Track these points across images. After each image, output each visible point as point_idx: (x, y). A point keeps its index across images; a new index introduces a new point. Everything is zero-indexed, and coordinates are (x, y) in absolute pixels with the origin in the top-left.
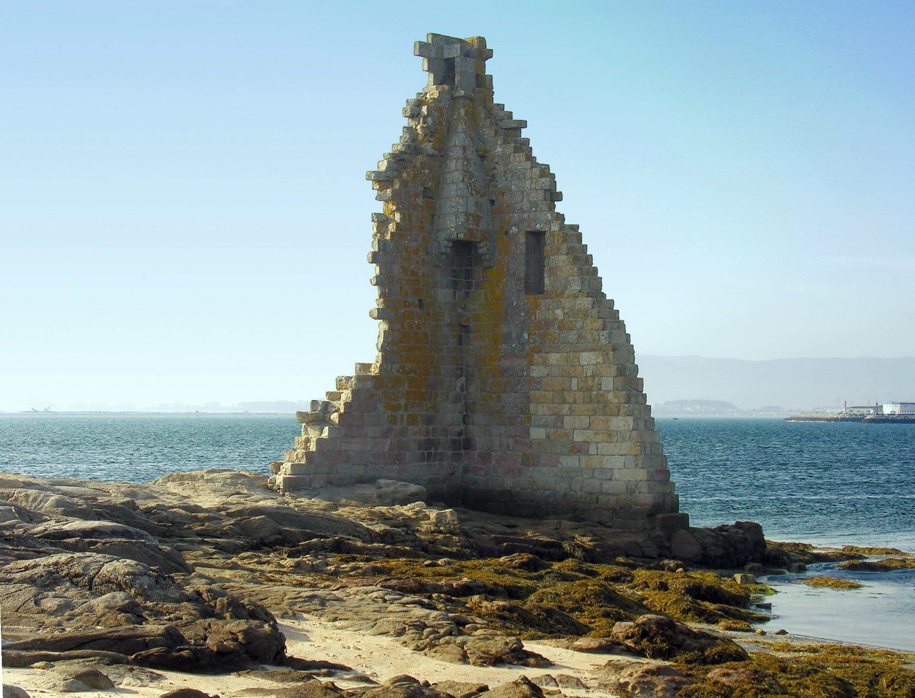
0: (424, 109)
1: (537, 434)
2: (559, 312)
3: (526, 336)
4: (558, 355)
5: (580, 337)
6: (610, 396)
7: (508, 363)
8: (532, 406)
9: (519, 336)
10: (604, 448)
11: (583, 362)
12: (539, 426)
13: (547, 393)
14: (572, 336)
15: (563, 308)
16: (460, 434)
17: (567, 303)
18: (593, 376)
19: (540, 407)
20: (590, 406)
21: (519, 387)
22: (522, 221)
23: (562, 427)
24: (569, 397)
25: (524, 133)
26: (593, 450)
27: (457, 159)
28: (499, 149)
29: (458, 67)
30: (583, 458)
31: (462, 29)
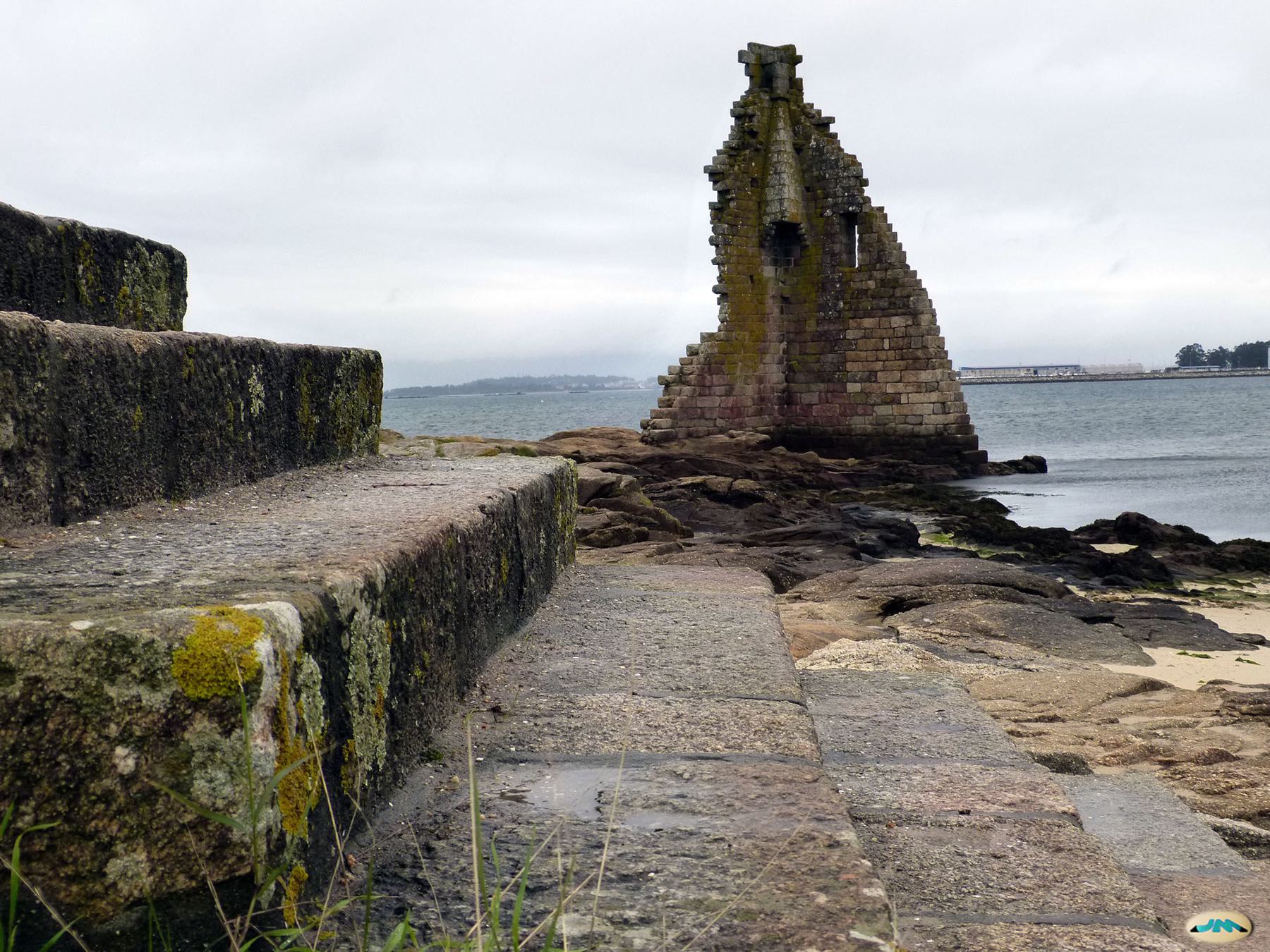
1: (853, 387)
5: (890, 304)
9: (836, 305)
10: (915, 397)
11: (894, 325)
14: (884, 303)
16: (783, 391)
17: (878, 275)
19: (855, 364)
22: (836, 204)
25: (833, 128)
26: (904, 399)
28: (813, 143)
29: (771, 71)
31: (775, 40)
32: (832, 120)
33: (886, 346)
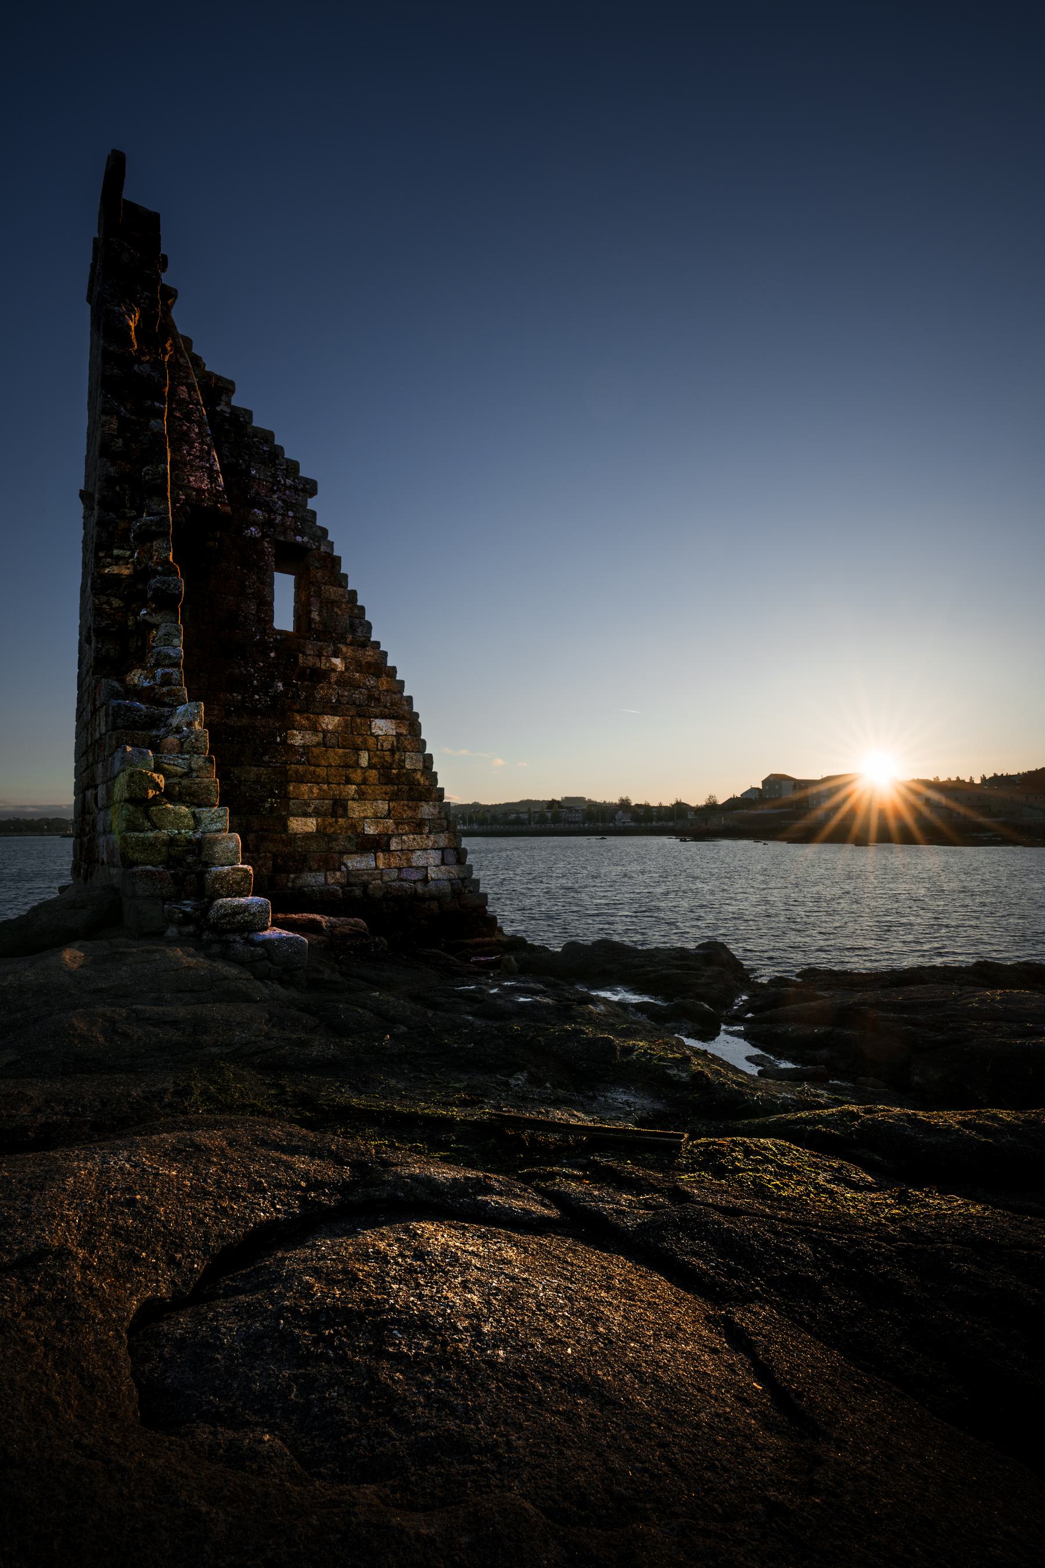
2: (337, 661)
3: (280, 684)
5: (371, 697)
6: (418, 776)
7: (245, 721)
12: (306, 815)
13: (318, 770)
15: (344, 658)
18: (392, 751)
19: (304, 788)
20: (389, 788)
21: (266, 758)
23: (345, 815)
24: (357, 776)
26: (394, 845)
30: (381, 855)
33: (364, 761)
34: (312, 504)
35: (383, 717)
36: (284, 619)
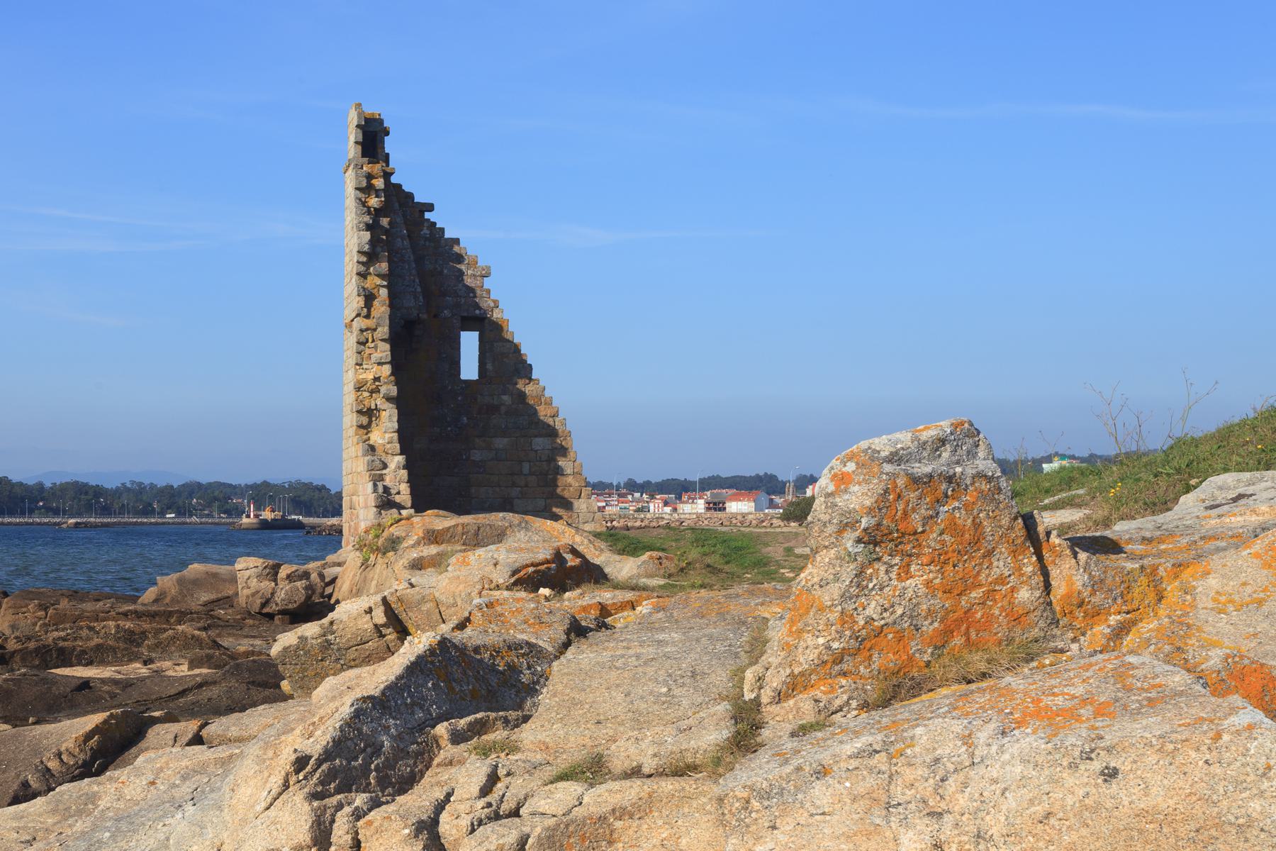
0: (379, 183)
2: (505, 398)
4: (506, 440)
8: (473, 490)
27: (403, 238)
32: (430, 207)
34: (487, 283)
35: (540, 436)
36: (469, 369)
